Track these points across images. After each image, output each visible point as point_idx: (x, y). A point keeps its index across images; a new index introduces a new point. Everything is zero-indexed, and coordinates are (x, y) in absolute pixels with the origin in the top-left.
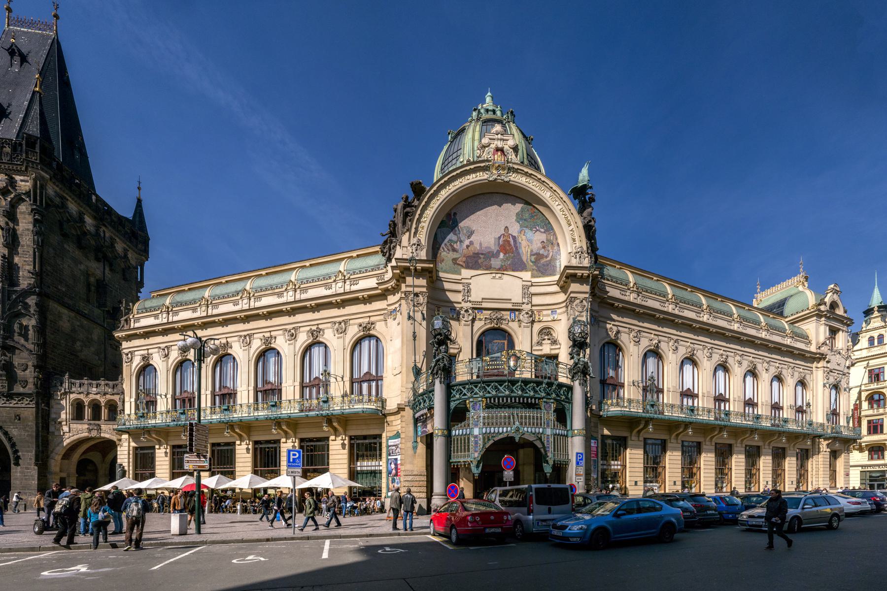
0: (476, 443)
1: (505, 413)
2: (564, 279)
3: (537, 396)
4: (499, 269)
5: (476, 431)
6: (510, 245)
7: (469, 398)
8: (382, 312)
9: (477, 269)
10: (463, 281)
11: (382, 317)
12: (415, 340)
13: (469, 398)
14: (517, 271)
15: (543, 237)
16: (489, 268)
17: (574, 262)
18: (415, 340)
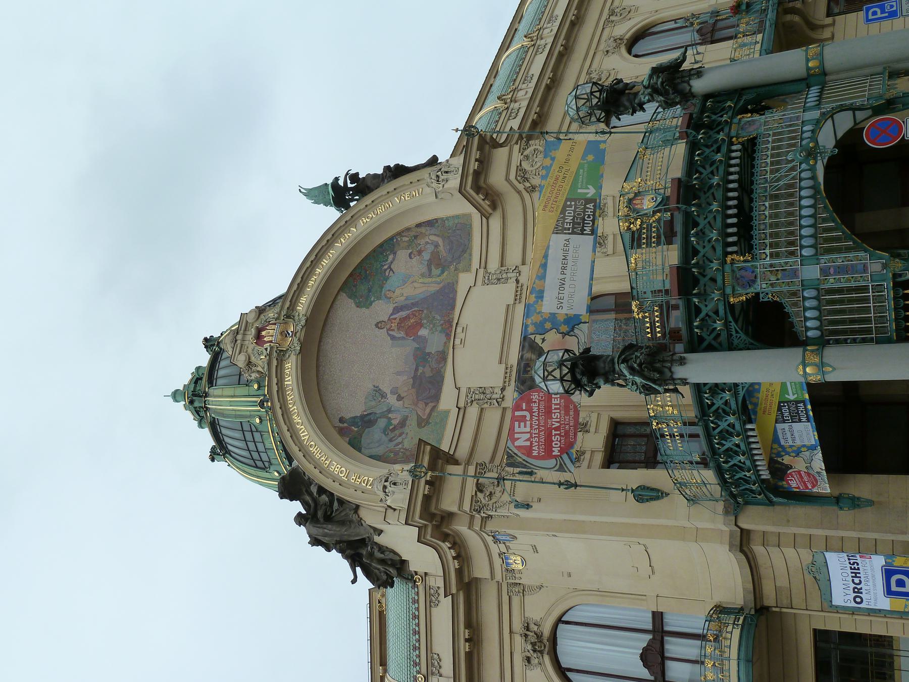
0: (840, 270)
1: (763, 210)
2: (479, 198)
3: (724, 149)
4: (448, 336)
5: (811, 272)
6: (407, 318)
7: (724, 295)
8: (505, 598)
9: (442, 378)
10: (461, 405)
11: (516, 600)
12: (576, 486)
13: (724, 295)
14: (454, 300)
15: (402, 254)
16: (442, 357)
17: (454, 182)
18: (576, 486)
